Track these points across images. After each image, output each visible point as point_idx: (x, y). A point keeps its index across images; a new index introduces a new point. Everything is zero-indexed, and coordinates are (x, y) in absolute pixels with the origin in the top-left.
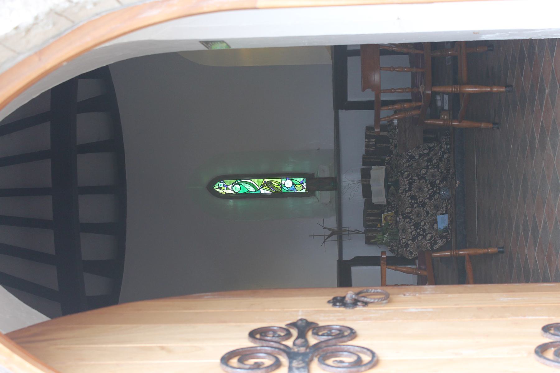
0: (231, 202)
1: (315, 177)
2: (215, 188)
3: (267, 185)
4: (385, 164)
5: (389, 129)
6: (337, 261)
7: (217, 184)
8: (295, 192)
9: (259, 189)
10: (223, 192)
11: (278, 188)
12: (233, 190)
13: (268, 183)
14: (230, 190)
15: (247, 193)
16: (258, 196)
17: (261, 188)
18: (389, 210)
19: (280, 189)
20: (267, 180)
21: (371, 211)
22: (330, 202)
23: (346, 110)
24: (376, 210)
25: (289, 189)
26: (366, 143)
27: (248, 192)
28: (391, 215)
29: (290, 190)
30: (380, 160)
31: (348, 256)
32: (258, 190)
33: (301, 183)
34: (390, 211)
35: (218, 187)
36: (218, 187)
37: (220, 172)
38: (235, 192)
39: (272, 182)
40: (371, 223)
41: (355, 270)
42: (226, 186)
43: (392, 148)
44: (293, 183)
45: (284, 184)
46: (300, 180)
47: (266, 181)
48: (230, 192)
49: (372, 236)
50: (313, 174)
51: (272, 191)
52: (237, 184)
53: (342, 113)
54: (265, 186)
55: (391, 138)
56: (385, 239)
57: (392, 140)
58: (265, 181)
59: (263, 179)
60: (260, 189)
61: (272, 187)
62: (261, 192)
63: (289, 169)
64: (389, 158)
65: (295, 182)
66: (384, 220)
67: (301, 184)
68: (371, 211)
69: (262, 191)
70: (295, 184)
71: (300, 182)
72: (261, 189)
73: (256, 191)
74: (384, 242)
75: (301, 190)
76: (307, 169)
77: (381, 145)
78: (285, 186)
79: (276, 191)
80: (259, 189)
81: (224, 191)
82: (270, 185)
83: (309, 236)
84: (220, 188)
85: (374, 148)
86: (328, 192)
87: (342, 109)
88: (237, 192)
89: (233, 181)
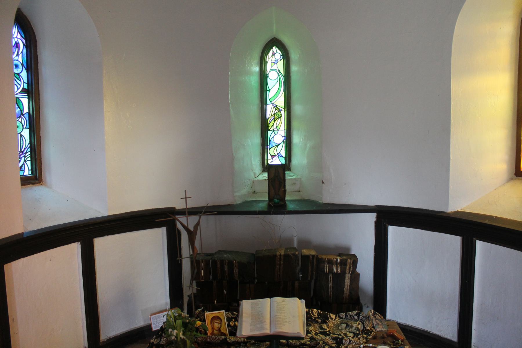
0: (256, 69)
1: (286, 173)
2: (274, 47)
3: (277, 113)
4: (308, 309)
5: (363, 317)
6: (174, 208)
7: (278, 51)
9: (272, 102)
10: (269, 59)
11: (273, 126)
12: (271, 70)
14: (272, 67)
15: (268, 88)
16: (263, 101)
17: (273, 105)
18: (231, 323)
19: (272, 129)
20: (283, 113)
21: (236, 266)
22: (255, 192)
24: (237, 273)
25: (272, 140)
26: (335, 260)
27: (268, 89)
28: (221, 329)
29: (270, 141)
30: (309, 279)
32: (271, 102)
33: (279, 154)
34: (229, 325)
35: (275, 53)
36: (275, 53)
37: (294, 56)
38: (268, 73)
40: (218, 266)
42: (276, 62)
43: (332, 319)
44: (279, 145)
45: (277, 134)
46: (283, 153)
47: (281, 111)
48: (269, 67)
50: (289, 169)
52: (279, 75)
53: (372, 217)
54: (275, 110)
55: (346, 316)
56: (175, 331)
57: (344, 318)
58: (282, 110)
59: (284, 108)
60: (272, 103)
61: (274, 118)
62: (268, 105)
63: (296, 139)
64: (316, 315)
65: (280, 147)
66: (214, 315)
67: (278, 154)
68: (236, 266)
70: (277, 147)
71: (279, 153)
73: (270, 99)
74: (170, 330)
75: (270, 155)
76: (295, 161)
77: (331, 282)
78: (275, 134)
79: (269, 123)
80: (272, 102)
81: (270, 58)
82: (276, 117)
83: (185, 191)
84: (274, 54)
85: (327, 272)
86: (267, 190)
87: (377, 217)
88: (268, 76)
89: (282, 72)
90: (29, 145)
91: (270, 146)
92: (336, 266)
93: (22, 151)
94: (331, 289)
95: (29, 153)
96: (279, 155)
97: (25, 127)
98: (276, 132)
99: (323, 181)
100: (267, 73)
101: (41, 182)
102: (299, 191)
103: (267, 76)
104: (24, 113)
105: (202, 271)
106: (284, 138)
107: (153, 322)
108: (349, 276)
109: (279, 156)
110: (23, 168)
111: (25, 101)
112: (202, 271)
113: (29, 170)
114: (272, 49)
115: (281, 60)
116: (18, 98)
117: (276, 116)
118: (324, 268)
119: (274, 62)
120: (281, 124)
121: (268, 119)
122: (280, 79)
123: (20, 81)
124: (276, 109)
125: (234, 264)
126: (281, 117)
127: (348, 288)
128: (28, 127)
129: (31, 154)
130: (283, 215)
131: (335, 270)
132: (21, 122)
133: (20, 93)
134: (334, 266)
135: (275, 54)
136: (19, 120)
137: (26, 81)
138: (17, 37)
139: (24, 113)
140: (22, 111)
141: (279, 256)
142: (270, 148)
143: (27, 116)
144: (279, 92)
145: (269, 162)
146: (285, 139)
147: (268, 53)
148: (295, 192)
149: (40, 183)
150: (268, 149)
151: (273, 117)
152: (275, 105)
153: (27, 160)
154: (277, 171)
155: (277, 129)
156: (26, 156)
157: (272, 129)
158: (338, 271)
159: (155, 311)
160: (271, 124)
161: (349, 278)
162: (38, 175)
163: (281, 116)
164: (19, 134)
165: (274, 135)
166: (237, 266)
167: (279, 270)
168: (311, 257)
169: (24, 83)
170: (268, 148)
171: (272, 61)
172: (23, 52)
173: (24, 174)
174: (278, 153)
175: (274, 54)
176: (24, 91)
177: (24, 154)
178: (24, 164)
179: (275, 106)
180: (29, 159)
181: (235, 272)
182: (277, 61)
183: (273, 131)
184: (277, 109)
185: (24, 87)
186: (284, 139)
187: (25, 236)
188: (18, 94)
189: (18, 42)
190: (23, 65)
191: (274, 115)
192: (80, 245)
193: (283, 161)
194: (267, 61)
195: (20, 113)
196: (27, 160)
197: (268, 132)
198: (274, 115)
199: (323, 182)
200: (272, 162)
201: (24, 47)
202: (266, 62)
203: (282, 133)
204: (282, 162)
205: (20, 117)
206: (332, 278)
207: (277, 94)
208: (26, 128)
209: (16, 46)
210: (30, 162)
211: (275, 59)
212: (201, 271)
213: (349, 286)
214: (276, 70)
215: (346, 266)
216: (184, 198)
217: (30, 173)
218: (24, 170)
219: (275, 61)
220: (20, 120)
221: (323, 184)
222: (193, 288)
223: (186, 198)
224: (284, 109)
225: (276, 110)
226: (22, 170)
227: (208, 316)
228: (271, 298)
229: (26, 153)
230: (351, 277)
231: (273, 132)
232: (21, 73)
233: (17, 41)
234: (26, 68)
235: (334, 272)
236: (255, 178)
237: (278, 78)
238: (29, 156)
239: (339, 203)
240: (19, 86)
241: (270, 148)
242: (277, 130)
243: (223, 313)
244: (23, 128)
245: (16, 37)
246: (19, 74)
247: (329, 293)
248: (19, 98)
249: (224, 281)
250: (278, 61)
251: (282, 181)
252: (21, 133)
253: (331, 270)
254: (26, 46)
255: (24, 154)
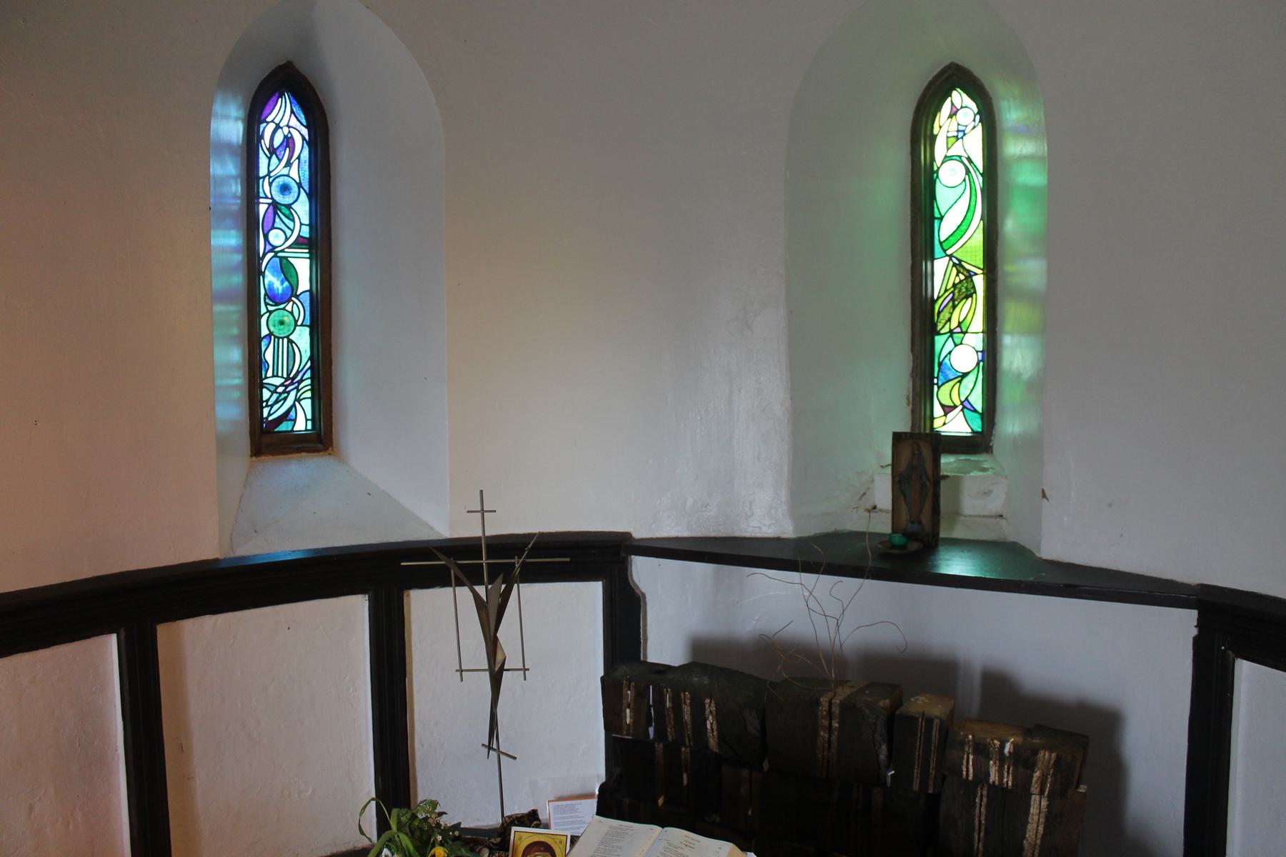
2: (954, 93)
3: (961, 281)
8: (935, 381)
9: (948, 252)
10: (940, 127)
11: (949, 320)
12: (947, 158)
13: (970, 286)
14: (948, 149)
15: (936, 210)
17: (950, 259)
19: (946, 329)
20: (979, 281)
22: (875, 507)
23: (1197, 641)
24: (715, 733)
25: (947, 360)
27: (937, 215)
29: (940, 364)
31: (643, 570)
33: (966, 404)
35: (959, 107)
36: (959, 107)
38: (938, 168)
39: (970, 299)
41: (593, 592)
44: (965, 375)
45: (961, 344)
47: (974, 278)
48: (940, 150)
49: (625, 704)
51: (938, 298)
52: (968, 172)
53: (1185, 622)
54: (957, 275)
58: (976, 274)
59: (982, 266)
60: (947, 255)
61: (953, 299)
62: (935, 261)
65: (969, 381)
66: (536, 839)
67: (962, 403)
69: (940, 266)
70: (960, 382)
71: (967, 399)
72: (947, 258)
73: (941, 243)
76: (1010, 425)
78: (956, 345)
79: (939, 313)
80: (949, 252)
81: (943, 125)
82: (963, 291)
84: (953, 114)
85: (970, 778)
87: (1200, 625)
88: (937, 177)
89: (979, 161)
90: (309, 362)
91: (941, 377)
92: (998, 764)
93: (291, 376)
94: (982, 834)
95: (309, 382)
96: (966, 405)
97: (299, 323)
98: (957, 337)
99: (1043, 491)
100: (935, 168)
101: (330, 449)
102: (1001, 516)
103: (935, 175)
104: (298, 293)
105: (628, 711)
106: (980, 354)
107: (555, 818)
108: (1044, 803)
109: (965, 410)
110: (292, 414)
111: (303, 266)
112: (628, 711)
113: (307, 420)
114: (949, 98)
115: (974, 127)
116: (286, 258)
117: (959, 291)
118: (962, 764)
119: (956, 134)
120: (973, 313)
121: (933, 302)
122: (972, 183)
123: (293, 220)
124: (958, 272)
125: (707, 706)
126: (974, 295)
127: (1038, 841)
128: (308, 322)
129: (312, 384)
130: (861, 580)
131: (994, 777)
132: (292, 313)
133: (290, 247)
134: (991, 762)
135: (958, 110)
136: (287, 308)
137: (306, 220)
138: (288, 126)
139: (298, 293)
140: (293, 288)
141: (827, 704)
142: (940, 384)
143: (306, 298)
144: (968, 222)
145: (937, 424)
146: (982, 360)
147: (939, 109)
148: (991, 517)
149: (326, 449)
150: (936, 387)
151: (952, 295)
152: (957, 259)
153: (301, 398)
154: (917, 452)
155: (961, 329)
156: (300, 388)
157: (948, 330)
158: (1005, 780)
159: (568, 792)
160: (945, 315)
161: (1044, 809)
162: (324, 428)
163: (972, 291)
164: (285, 340)
165: (953, 346)
166: (714, 713)
167: (826, 745)
168: (921, 723)
169: (301, 224)
170: (933, 384)
171: (948, 132)
172: (302, 156)
173: (295, 429)
174: (963, 399)
175: (954, 110)
176: (299, 243)
177: (296, 384)
178: (294, 405)
179: (957, 262)
180: (309, 394)
181: (709, 726)
182: (964, 131)
183: (949, 334)
184: (962, 270)
185: (301, 234)
186: (980, 358)
187: (223, 565)
188: (286, 250)
189: (289, 135)
190: (300, 185)
191: (954, 290)
192: (367, 602)
193: (978, 427)
194: (935, 132)
195: (290, 292)
196: (301, 398)
197: (937, 338)
198: (952, 289)
199: (1044, 496)
200: (944, 424)
201: (305, 145)
202: (933, 138)
203: (975, 340)
204: (972, 426)
205: (289, 300)
206: (985, 799)
207: (963, 228)
208: (302, 325)
209: (285, 144)
210: (310, 401)
211: (959, 124)
212: (625, 710)
213: (1039, 836)
214: (960, 157)
215: (1033, 771)
216: (483, 514)
217: (309, 427)
218: (295, 420)
219: (958, 131)
220: (289, 308)
221: (1045, 500)
222: (500, 753)
223: (483, 511)
224: (982, 272)
225: (960, 275)
226: (291, 420)
227: (520, 839)
228: (666, 827)
229: (302, 380)
230: (1048, 806)
231: (950, 339)
232: (293, 203)
233: (289, 132)
234: (308, 192)
235: (991, 781)
236: (881, 469)
237: (964, 180)
238: (309, 387)
239: (1088, 565)
240: (289, 233)
241: (940, 384)
242: (962, 332)
243: (564, 838)
244: (296, 325)
245: (286, 124)
246: (289, 207)
247: (974, 845)
248: (289, 259)
249: (683, 749)
250: (966, 132)
251: (928, 483)
252: (291, 337)
253: (982, 775)
254: (311, 143)
255: (296, 384)
